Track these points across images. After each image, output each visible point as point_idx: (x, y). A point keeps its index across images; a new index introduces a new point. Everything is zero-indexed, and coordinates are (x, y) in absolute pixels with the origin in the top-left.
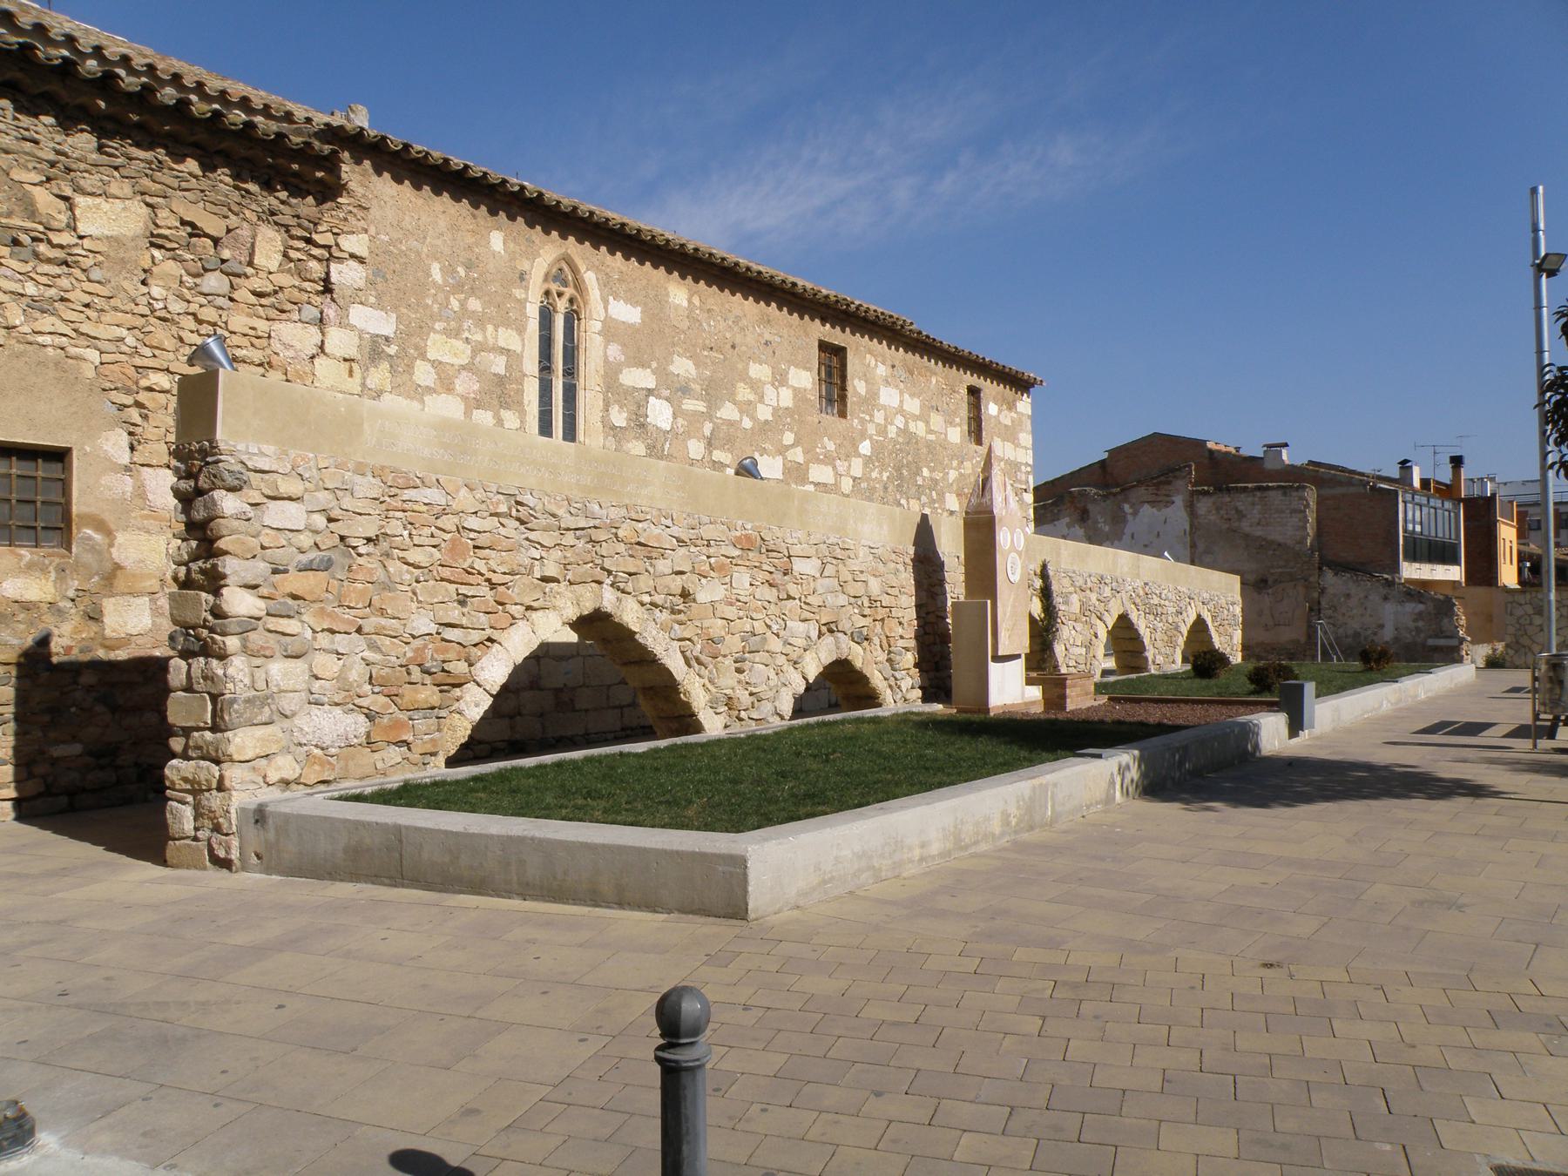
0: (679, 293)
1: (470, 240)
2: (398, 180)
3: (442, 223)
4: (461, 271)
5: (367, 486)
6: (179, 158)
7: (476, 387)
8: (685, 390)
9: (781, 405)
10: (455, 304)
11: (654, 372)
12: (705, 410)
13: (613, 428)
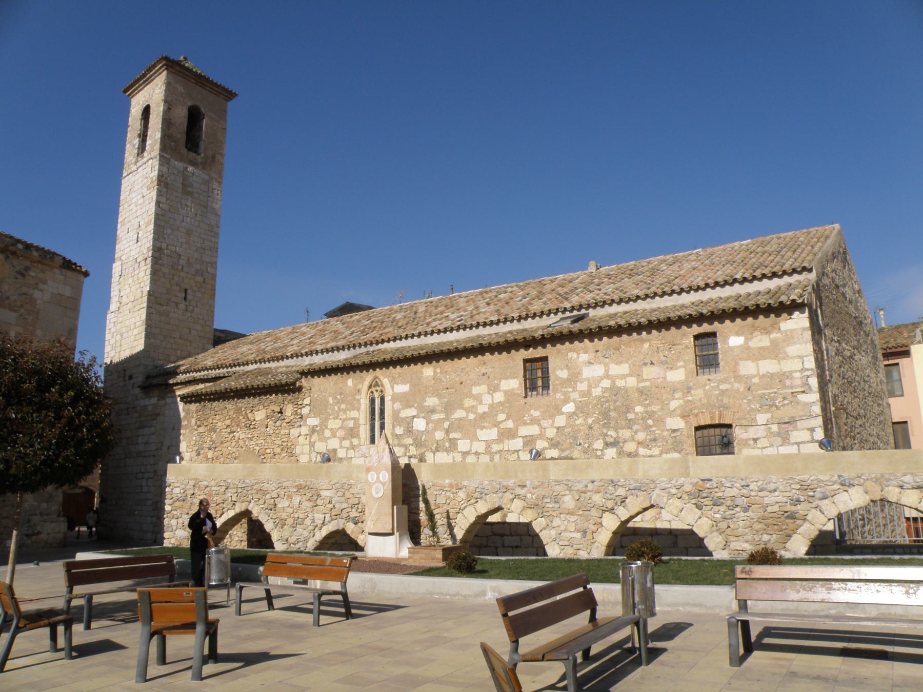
0: (428, 371)
1: (341, 385)
4: (338, 397)
5: (192, 483)
6: (271, 395)
7: (343, 433)
8: (433, 411)
9: (495, 402)
10: (336, 408)
11: (416, 408)
12: (444, 417)
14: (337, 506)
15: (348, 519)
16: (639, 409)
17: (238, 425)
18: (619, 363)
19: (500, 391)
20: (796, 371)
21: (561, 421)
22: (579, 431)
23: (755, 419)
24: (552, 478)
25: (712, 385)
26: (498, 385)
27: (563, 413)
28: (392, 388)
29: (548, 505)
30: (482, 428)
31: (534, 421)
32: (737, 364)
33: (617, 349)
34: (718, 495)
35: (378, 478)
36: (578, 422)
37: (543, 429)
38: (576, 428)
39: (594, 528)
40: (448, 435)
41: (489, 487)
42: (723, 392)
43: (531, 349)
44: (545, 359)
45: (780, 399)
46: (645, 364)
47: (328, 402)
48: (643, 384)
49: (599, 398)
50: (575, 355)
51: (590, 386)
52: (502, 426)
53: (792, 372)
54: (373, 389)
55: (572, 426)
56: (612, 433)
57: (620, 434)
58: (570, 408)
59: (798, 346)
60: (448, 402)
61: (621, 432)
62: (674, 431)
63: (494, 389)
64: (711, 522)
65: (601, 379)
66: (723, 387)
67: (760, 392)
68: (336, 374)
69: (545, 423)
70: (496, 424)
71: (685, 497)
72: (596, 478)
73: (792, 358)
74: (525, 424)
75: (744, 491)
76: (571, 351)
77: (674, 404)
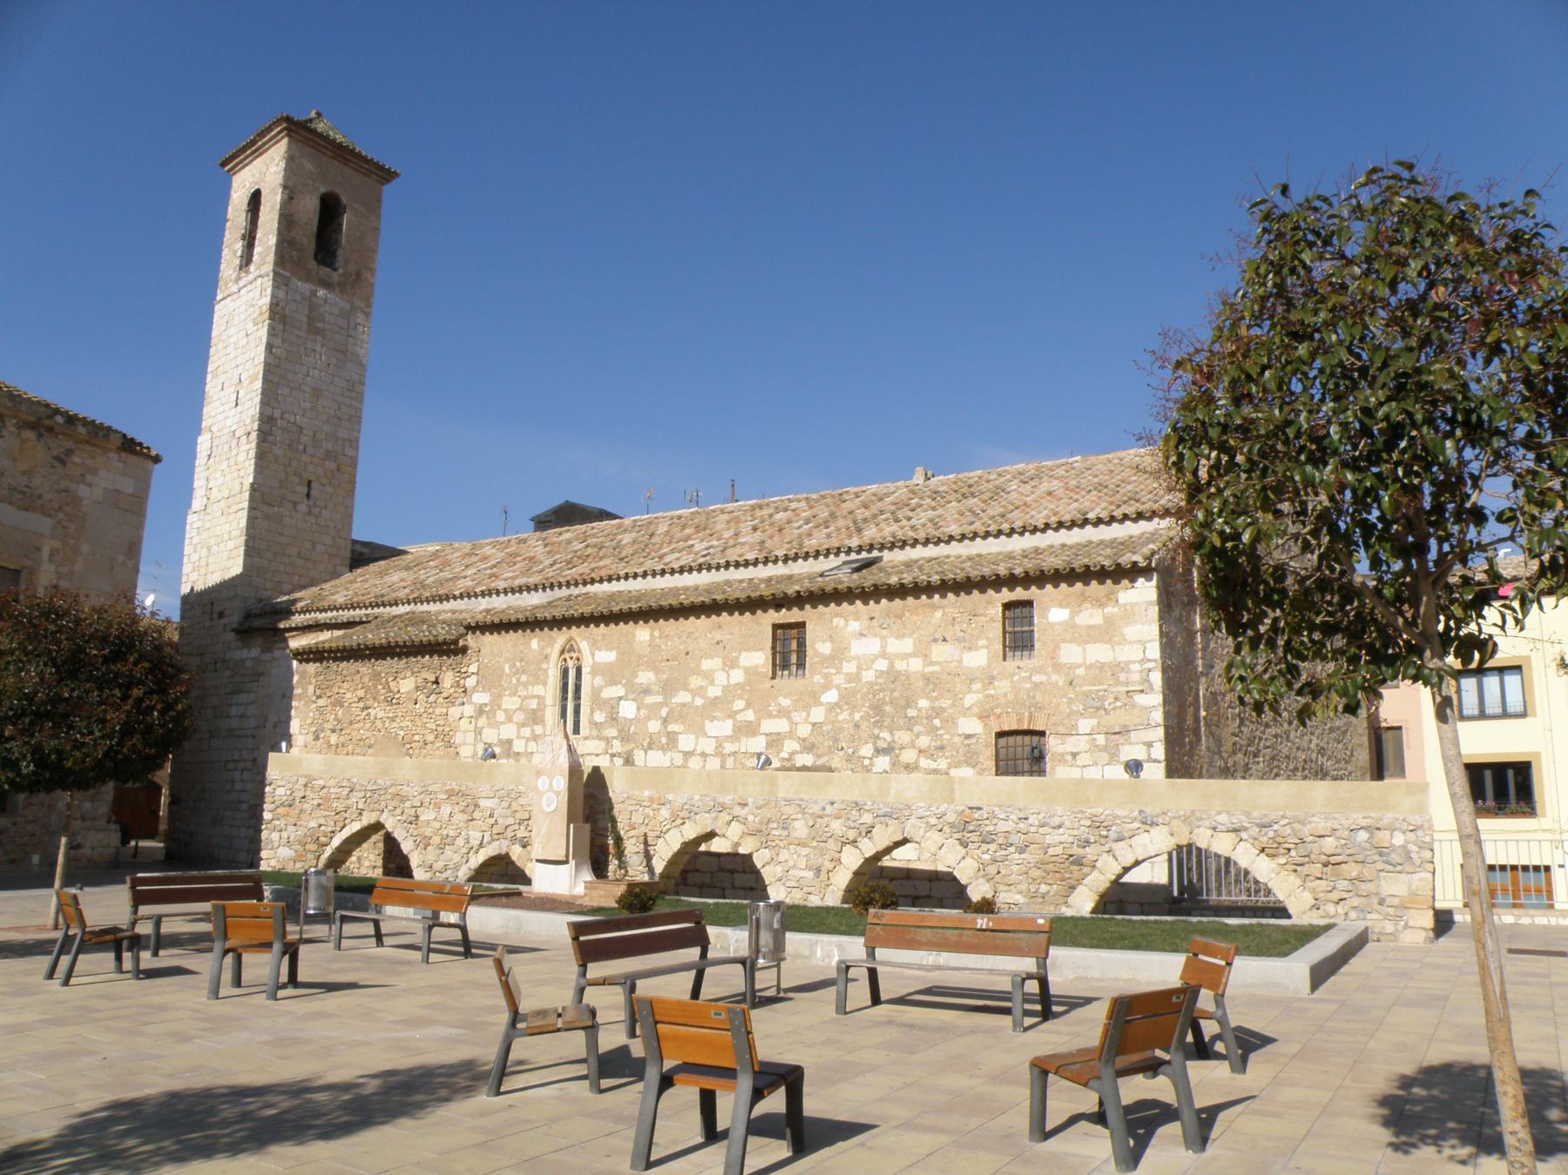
0: (642, 633)
2: (492, 634)
3: (509, 645)
5: (302, 781)
8: (647, 691)
10: (514, 681)
13: (596, 724)
14: (500, 821)
15: (514, 839)
16: (923, 703)
17: (375, 698)
18: (901, 636)
19: (739, 667)
20: (1134, 662)
21: (818, 714)
22: (842, 729)
23: (1075, 727)
24: (781, 795)
25: (1023, 674)
26: (737, 658)
27: (821, 704)
28: (593, 655)
29: (774, 832)
30: (713, 719)
31: (783, 713)
32: (1057, 647)
33: (899, 617)
34: (988, 829)
35: (551, 785)
36: (840, 718)
37: (794, 724)
38: (838, 725)
39: (830, 865)
40: (666, 727)
41: (700, 804)
42: (1037, 686)
43: (784, 610)
44: (801, 626)
45: (1111, 700)
46: (935, 640)
47: (503, 670)
48: (930, 669)
49: (871, 685)
50: (842, 622)
51: (859, 668)
52: (739, 717)
53: (1129, 663)
54: (567, 655)
55: (832, 723)
56: (885, 735)
57: (896, 738)
58: (831, 696)
59: (1139, 627)
60: (667, 681)
61: (898, 734)
62: (968, 737)
63: (731, 664)
64: (976, 865)
65: (876, 658)
66: (1037, 678)
67: (1085, 688)
68: (516, 631)
69: (796, 716)
70: (732, 715)
71: (947, 829)
72: (836, 799)
73: (1131, 643)
74: (770, 716)
75: (1022, 825)
76: (838, 615)
77: (970, 699)
